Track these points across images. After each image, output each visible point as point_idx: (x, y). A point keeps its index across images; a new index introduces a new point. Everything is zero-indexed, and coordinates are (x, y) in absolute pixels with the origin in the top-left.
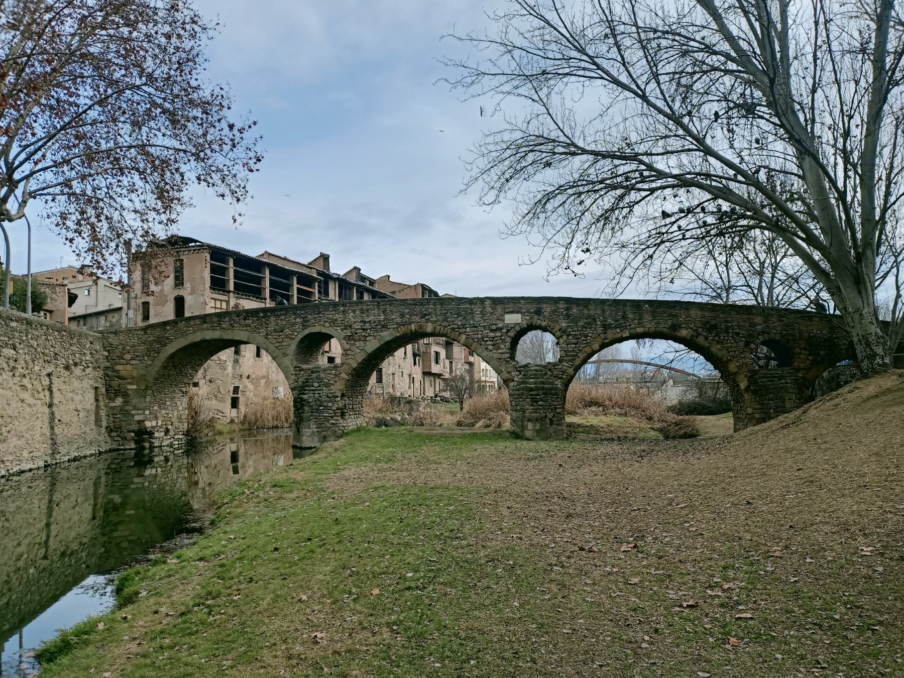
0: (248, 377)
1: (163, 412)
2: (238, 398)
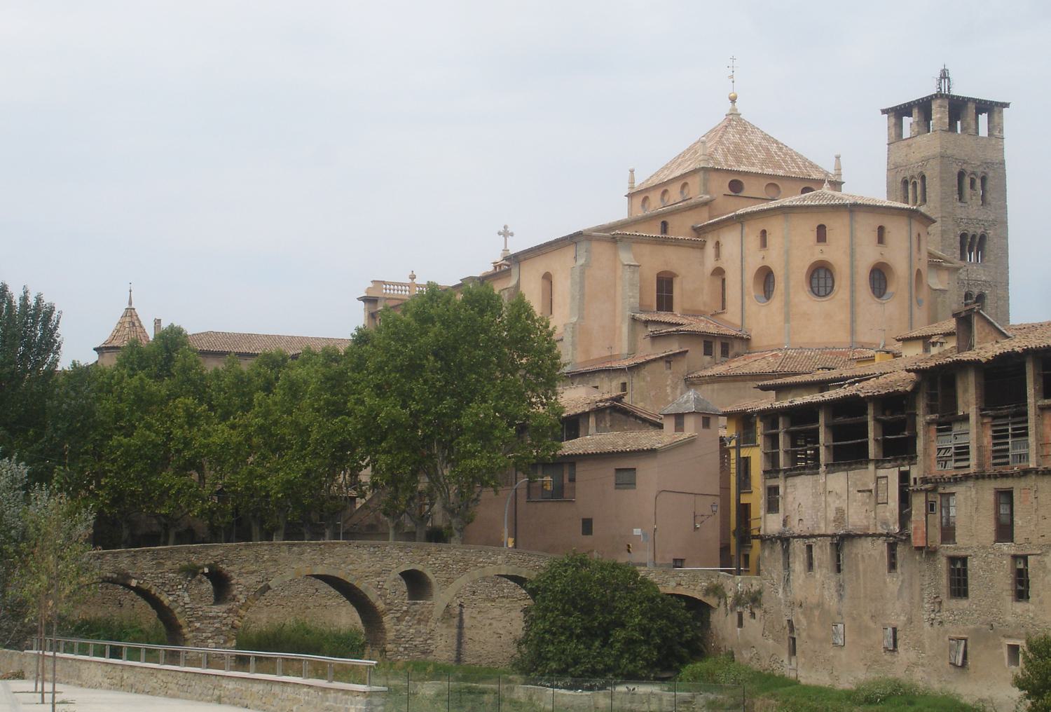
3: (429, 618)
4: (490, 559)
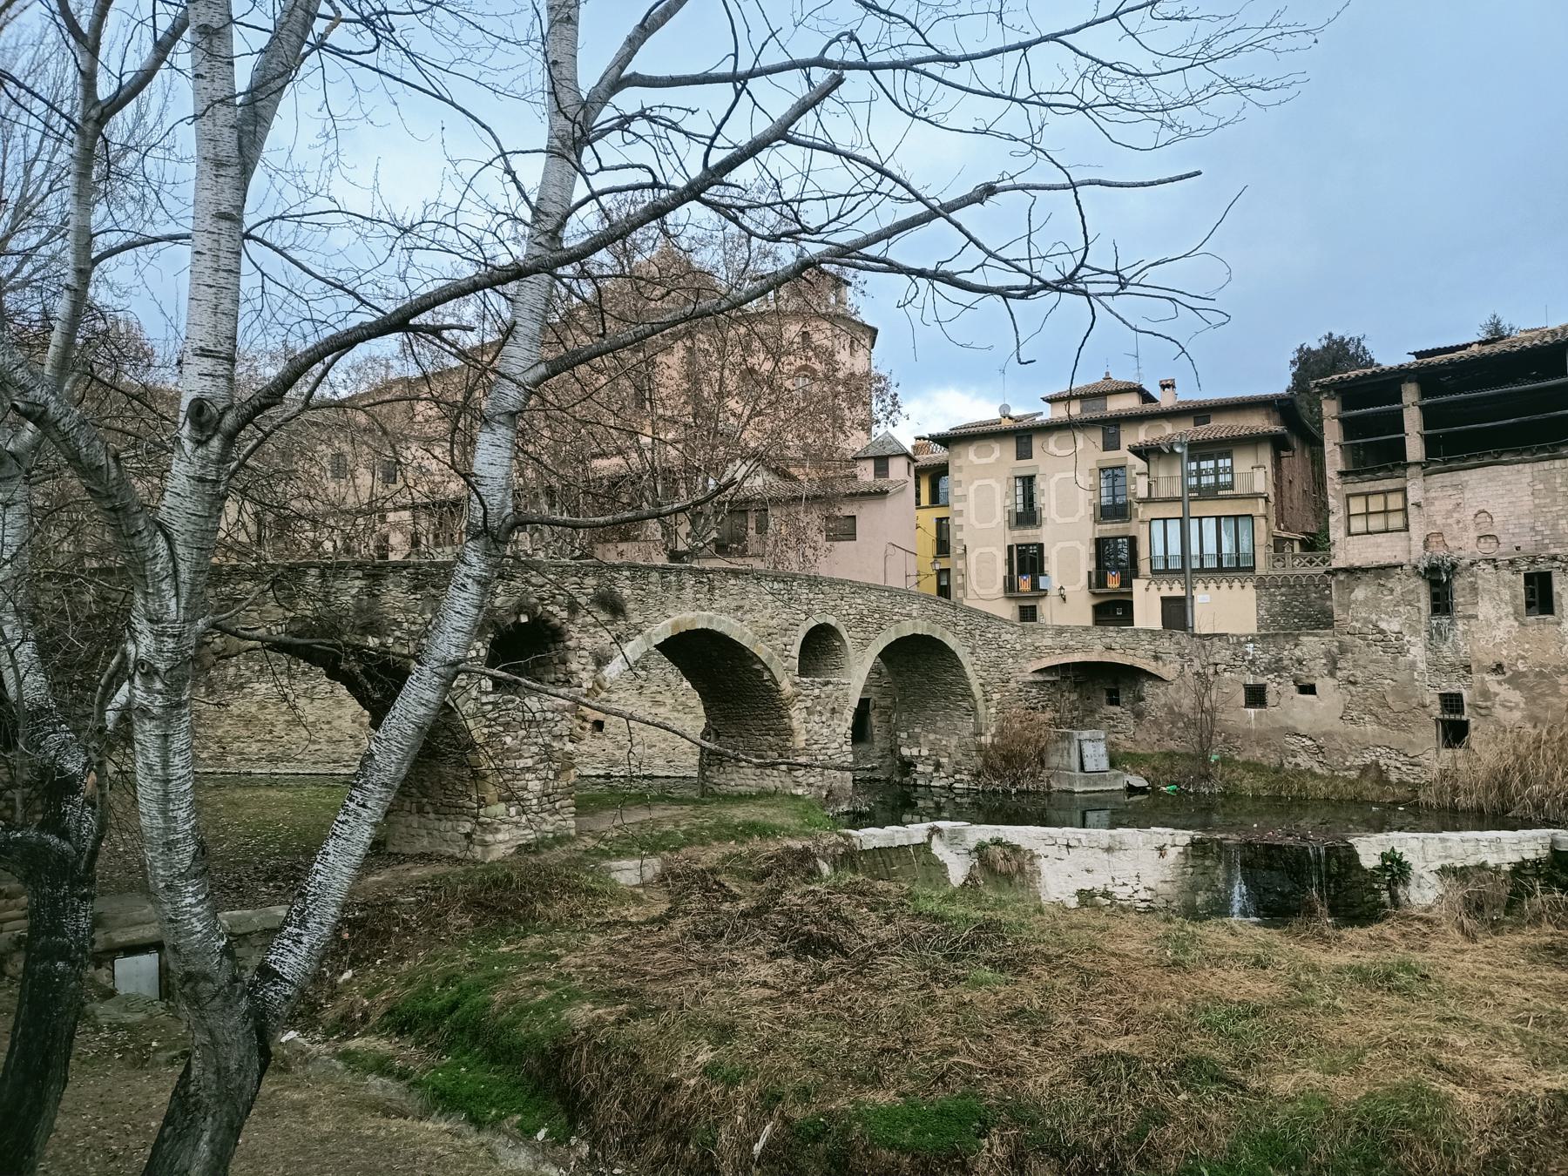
0: (1498, 669)
1: (932, 737)
2: (1466, 723)
3: (844, 708)
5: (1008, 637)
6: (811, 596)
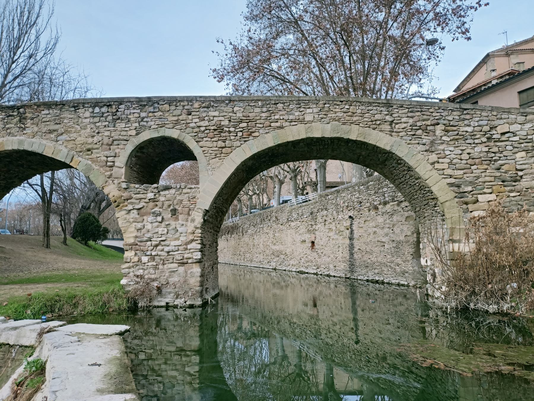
4: (293, 114)
5: (515, 128)
6: (143, 115)
